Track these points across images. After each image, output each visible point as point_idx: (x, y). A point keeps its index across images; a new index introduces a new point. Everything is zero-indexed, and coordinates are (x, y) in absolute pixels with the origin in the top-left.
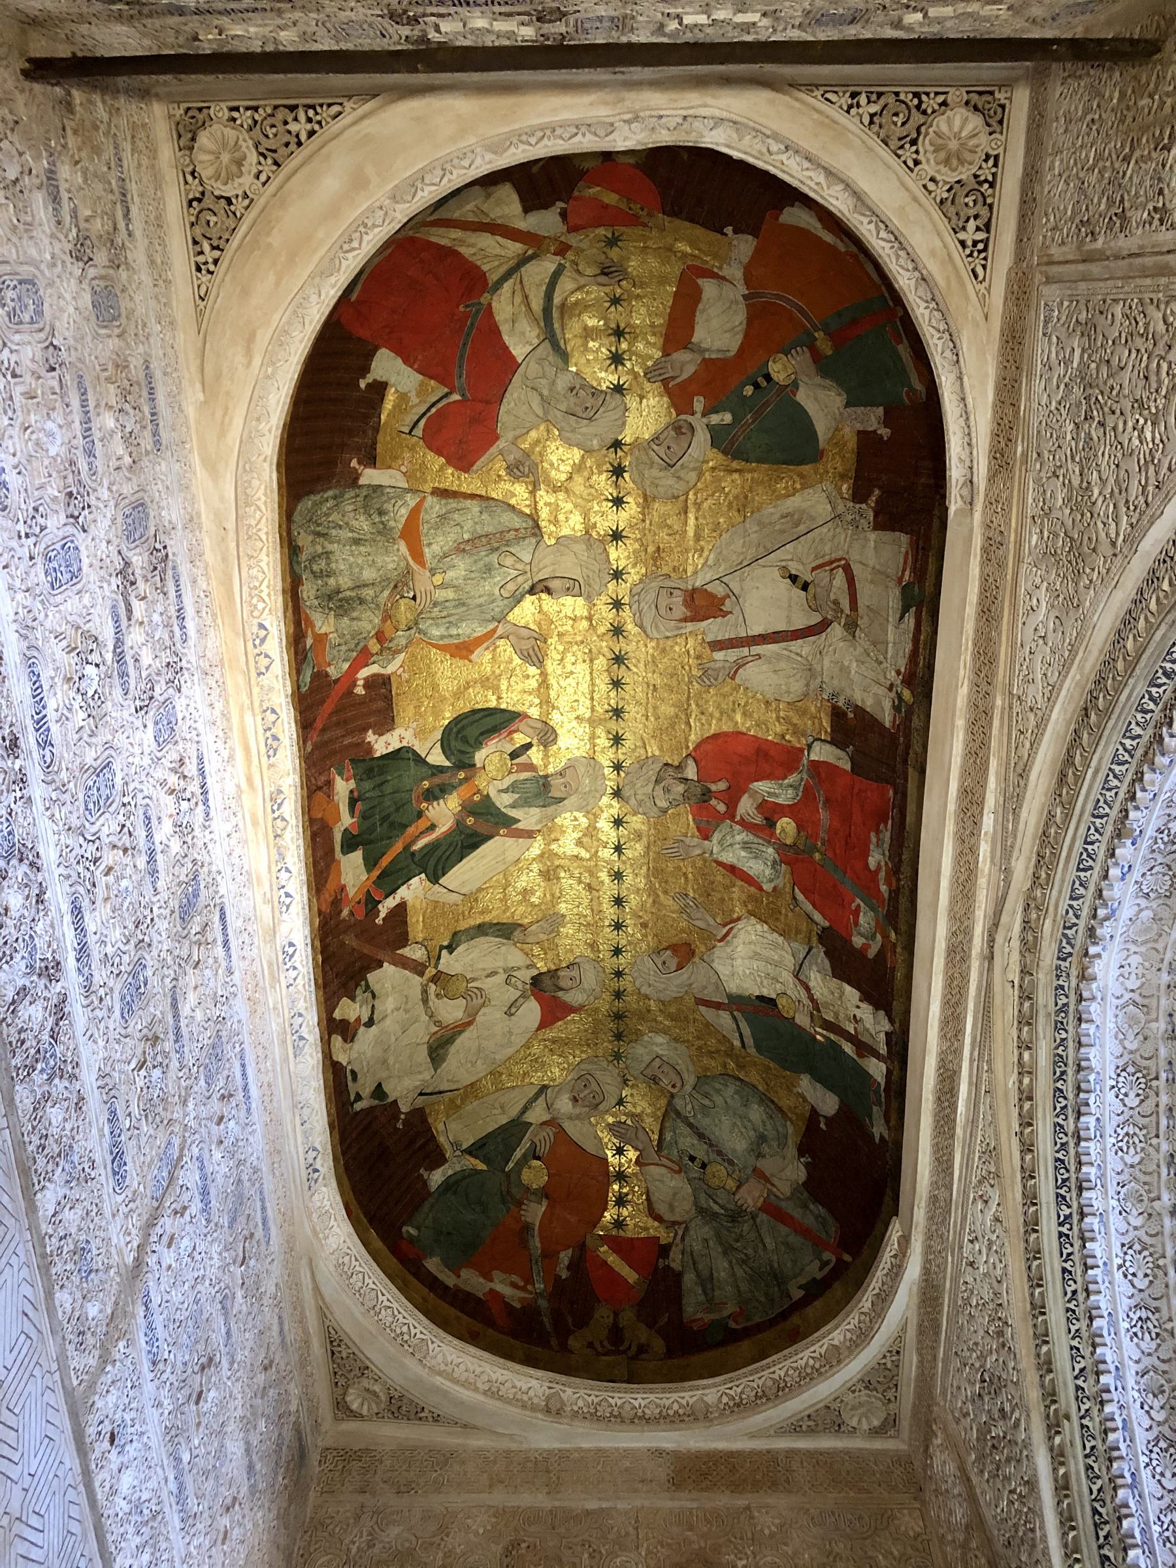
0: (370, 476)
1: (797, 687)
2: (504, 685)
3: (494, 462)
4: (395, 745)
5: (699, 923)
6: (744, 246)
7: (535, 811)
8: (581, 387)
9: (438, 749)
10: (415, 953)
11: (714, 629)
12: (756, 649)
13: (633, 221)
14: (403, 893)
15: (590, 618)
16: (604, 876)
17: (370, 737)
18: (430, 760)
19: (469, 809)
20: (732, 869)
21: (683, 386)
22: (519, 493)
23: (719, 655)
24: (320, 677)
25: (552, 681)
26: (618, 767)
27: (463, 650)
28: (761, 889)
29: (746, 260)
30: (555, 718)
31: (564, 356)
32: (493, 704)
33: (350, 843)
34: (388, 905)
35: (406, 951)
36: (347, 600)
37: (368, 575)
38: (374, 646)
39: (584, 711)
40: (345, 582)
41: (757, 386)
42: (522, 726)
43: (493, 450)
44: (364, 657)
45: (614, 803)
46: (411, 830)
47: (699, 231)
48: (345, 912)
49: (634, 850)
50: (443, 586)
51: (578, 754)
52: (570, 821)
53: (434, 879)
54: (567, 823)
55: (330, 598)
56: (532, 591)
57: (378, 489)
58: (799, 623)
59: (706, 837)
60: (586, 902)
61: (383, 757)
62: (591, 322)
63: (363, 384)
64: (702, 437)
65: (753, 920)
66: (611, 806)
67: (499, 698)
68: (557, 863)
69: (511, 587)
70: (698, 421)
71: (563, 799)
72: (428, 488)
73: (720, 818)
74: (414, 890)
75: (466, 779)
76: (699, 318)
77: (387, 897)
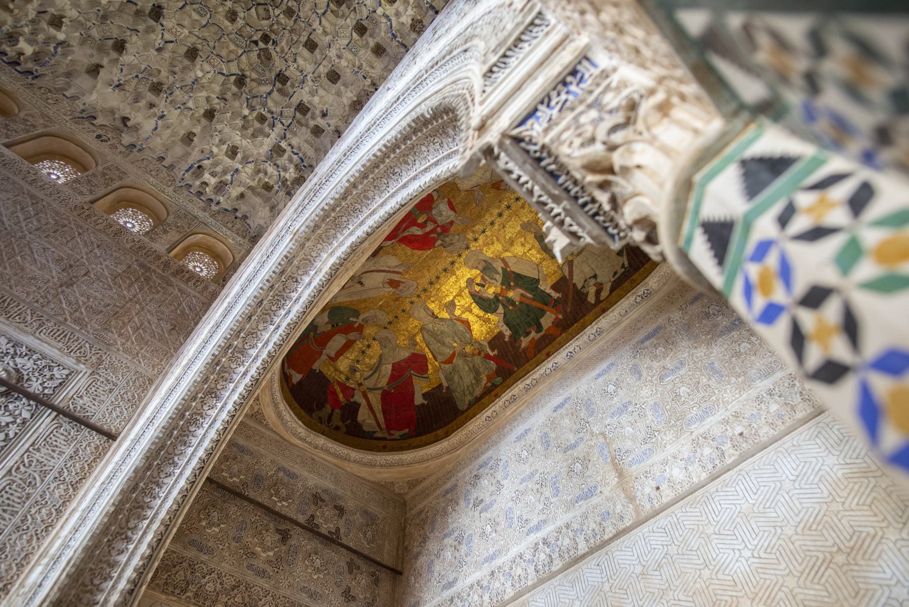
0: (445, 384)
1: (382, 259)
2: (466, 305)
3: (417, 350)
4: (505, 327)
5: (481, 193)
6: (316, 366)
7: (495, 265)
8: (383, 346)
9: (498, 311)
10: (566, 268)
11: (396, 277)
12: (388, 269)
13: (339, 383)
14: (548, 291)
15: (429, 299)
16: (496, 227)
17: (507, 339)
18: (503, 312)
19: (509, 288)
20: (452, 208)
21: (357, 331)
22: (418, 339)
23: (401, 270)
24: (498, 373)
25: (454, 294)
26: (460, 256)
27: (467, 323)
28: (449, 200)
29: (318, 361)
30: (463, 284)
31: (381, 356)
32: (474, 304)
33: (539, 328)
34: (555, 295)
35: (567, 274)
36: (475, 372)
37: (467, 369)
38: (483, 354)
39: (453, 279)
40: (472, 377)
41: (337, 325)
42: (473, 291)
43: (416, 352)
44: (488, 356)
45: (471, 246)
46: (527, 302)
47: (325, 372)
48: (560, 317)
49: (479, 228)
50: (456, 342)
51: (468, 270)
52: (489, 253)
53: (538, 281)
54: (490, 253)
55: (477, 380)
56: (437, 317)
57: (446, 379)
58: (368, 274)
59: (452, 223)
60: (510, 223)
61: (510, 330)
62: (367, 360)
63: (426, 402)
64: (361, 317)
65: (461, 189)
66: (473, 246)
67: (471, 304)
68: (505, 245)
69: (441, 323)
70: (360, 320)
71: (485, 261)
72: (436, 363)
73: (442, 227)
74: (545, 287)
75: (500, 295)
76: (341, 346)
77: (551, 296)
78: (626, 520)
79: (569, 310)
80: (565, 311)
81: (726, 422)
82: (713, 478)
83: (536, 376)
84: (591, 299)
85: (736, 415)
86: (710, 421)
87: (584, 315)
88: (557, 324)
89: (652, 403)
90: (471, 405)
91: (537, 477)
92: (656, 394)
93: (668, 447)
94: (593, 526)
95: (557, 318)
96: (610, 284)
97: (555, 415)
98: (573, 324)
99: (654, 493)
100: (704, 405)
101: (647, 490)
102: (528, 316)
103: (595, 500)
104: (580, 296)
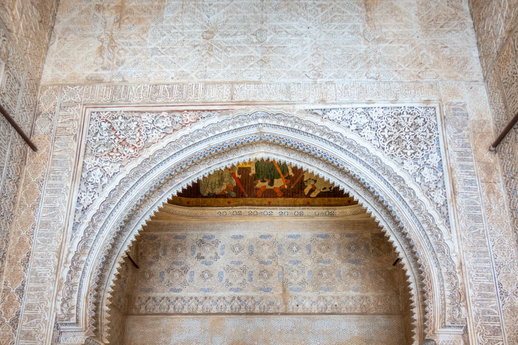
33: (271, 183)
36: (221, 178)
48: (286, 187)
55: (220, 184)
77: (288, 172)
78: (280, 310)
79: (292, 187)
80: (290, 187)
81: (333, 297)
82: (319, 314)
83: (259, 211)
84: (306, 191)
85: (338, 298)
86: (328, 293)
87: (298, 197)
88: (282, 189)
89: (310, 269)
90: (209, 196)
91: (241, 266)
92: (313, 266)
93: (308, 293)
94: (264, 304)
95: (284, 186)
96: (319, 192)
97: (260, 239)
98: (290, 197)
99: (295, 307)
100: (329, 286)
101: (293, 304)
102: (270, 172)
103: (268, 294)
104: (302, 185)
